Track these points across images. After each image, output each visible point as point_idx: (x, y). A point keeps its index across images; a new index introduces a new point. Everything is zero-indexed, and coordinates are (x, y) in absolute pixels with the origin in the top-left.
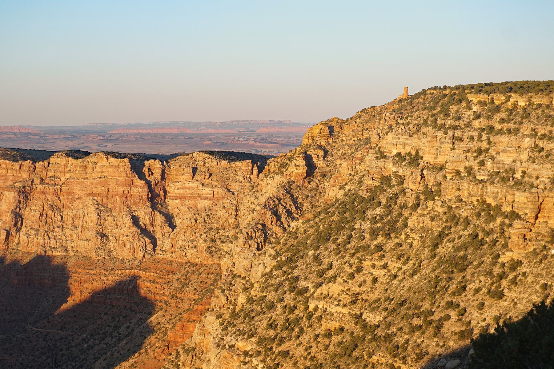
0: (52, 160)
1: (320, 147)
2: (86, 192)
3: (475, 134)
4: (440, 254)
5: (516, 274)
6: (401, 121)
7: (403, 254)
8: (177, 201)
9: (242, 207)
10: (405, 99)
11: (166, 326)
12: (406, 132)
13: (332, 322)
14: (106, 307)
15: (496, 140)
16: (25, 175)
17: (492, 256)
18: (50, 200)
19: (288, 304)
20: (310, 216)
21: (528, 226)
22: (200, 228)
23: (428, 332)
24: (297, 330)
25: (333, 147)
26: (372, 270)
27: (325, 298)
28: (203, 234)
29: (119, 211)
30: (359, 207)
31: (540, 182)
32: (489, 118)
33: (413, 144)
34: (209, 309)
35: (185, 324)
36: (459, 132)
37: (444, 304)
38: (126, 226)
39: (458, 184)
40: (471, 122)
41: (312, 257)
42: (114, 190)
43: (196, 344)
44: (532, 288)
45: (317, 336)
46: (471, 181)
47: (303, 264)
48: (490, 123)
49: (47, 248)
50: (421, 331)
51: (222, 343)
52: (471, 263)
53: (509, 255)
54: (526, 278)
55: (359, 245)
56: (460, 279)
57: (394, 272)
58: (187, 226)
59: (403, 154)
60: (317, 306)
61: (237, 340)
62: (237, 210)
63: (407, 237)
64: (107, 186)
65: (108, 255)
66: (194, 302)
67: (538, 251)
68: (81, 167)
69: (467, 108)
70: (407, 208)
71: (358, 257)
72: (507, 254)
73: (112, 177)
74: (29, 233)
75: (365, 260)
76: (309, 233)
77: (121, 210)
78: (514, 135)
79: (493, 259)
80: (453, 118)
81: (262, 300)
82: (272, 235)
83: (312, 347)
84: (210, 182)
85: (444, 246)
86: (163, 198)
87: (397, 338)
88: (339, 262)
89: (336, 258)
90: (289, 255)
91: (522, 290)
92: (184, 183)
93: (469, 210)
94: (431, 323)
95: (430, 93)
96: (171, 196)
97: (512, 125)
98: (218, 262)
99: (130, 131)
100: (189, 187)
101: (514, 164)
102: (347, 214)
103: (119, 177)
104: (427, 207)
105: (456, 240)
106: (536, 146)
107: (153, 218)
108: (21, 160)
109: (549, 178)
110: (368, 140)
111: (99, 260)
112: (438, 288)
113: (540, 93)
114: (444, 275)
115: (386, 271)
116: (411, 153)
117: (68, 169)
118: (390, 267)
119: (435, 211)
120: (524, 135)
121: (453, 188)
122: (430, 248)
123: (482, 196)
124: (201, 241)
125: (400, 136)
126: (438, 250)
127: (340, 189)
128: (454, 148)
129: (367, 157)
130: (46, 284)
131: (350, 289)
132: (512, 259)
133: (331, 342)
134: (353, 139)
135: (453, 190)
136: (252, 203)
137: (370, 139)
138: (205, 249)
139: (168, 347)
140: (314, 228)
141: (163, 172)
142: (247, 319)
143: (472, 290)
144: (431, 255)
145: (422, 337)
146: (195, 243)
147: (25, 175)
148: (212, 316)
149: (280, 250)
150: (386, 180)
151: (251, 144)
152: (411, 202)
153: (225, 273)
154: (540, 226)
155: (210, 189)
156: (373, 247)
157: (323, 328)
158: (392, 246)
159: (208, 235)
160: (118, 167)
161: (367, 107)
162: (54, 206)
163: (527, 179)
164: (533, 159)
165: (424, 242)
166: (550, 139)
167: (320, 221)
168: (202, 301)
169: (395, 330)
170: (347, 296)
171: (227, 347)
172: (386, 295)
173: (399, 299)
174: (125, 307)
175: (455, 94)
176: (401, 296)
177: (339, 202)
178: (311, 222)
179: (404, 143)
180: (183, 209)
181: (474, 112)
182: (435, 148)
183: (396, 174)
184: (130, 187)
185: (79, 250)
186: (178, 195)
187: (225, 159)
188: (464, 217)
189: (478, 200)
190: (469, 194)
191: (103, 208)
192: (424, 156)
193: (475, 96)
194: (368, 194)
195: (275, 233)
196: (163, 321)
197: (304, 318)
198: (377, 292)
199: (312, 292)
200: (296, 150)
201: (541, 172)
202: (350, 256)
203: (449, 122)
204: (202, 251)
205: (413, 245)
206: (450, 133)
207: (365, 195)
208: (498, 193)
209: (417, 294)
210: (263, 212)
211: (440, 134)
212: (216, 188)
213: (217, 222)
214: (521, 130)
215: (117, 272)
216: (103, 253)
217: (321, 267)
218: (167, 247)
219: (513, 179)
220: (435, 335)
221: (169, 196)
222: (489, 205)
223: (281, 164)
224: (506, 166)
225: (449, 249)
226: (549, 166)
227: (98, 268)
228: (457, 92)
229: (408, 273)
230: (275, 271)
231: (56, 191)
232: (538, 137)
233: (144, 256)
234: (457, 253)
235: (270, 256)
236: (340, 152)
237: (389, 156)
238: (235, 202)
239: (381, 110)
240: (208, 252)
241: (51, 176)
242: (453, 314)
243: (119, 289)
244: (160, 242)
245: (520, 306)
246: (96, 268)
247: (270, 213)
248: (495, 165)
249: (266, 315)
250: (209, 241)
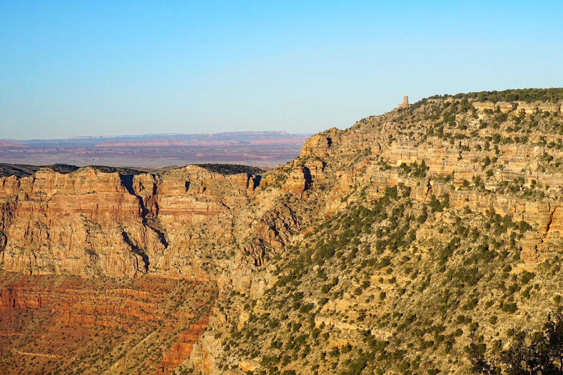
0: (38, 175)
1: (318, 158)
2: (74, 208)
3: (482, 143)
4: (450, 267)
5: (528, 286)
6: (404, 131)
7: (411, 268)
8: (170, 216)
9: (239, 222)
10: (405, 108)
11: (161, 347)
12: (411, 142)
13: (340, 339)
14: (96, 328)
15: (504, 149)
16: (8, 191)
17: (503, 268)
18: (36, 217)
19: (294, 322)
20: (311, 229)
21: (539, 237)
22: (195, 244)
23: (440, 348)
24: (303, 348)
25: (332, 158)
26: (380, 285)
27: (331, 314)
28: (198, 250)
29: (109, 228)
30: (364, 219)
31: (551, 191)
32: (496, 127)
33: (419, 154)
34: (207, 328)
35: (181, 344)
36: (466, 141)
37: (456, 318)
38: (116, 243)
39: (466, 194)
40: (477, 131)
41: (317, 272)
42: (104, 206)
43: (194, 365)
44: (546, 300)
45: (324, 354)
46: (480, 191)
47: (308, 280)
48: (497, 131)
49: (33, 268)
50: (433, 347)
51: (224, 364)
52: (482, 276)
53: (521, 267)
54: (539, 290)
55: (366, 259)
56: (471, 293)
57: (402, 286)
58: (182, 243)
59: (408, 165)
60: (323, 323)
61: (240, 360)
62: (233, 225)
63: (416, 250)
64: (96, 201)
65: (98, 274)
66: (189, 321)
67: (550, 262)
68: (68, 182)
69: (473, 117)
70: (414, 220)
71: (365, 272)
72: (519, 265)
73: (102, 192)
74: (13, 251)
75: (372, 274)
76: (311, 247)
77: (111, 226)
78: (523, 144)
79: (504, 271)
80: (459, 127)
81: (266, 318)
82: (270, 250)
83: (319, 366)
84: (205, 196)
85: (453, 259)
86: (155, 213)
87: (408, 355)
88: (345, 277)
89: (341, 273)
90: (293, 270)
91: (535, 302)
92: (178, 198)
93: (478, 221)
94: (442, 338)
95: (431, 102)
96: (163, 211)
97: (520, 133)
98: (215, 279)
99: (119, 144)
100: (183, 202)
101: (523, 173)
102: (352, 227)
103: (108, 192)
104: (435, 219)
105: (466, 252)
106: (546, 154)
107: (144, 234)
108: (5, 175)
109: (560, 187)
110: (368, 151)
111: (88, 279)
112: (449, 302)
113: (547, 101)
114: (455, 289)
115: (394, 285)
116: (417, 163)
117: (55, 185)
118: (399, 281)
119: (443, 223)
120: (532, 144)
121: (461, 198)
122: (439, 261)
123: (491, 206)
124: (196, 258)
125: (405, 146)
126: (448, 263)
127: (342, 202)
128: (460, 158)
129: (370, 168)
130: (32, 305)
131: (357, 305)
132: (524, 272)
133: (338, 360)
134: (352, 150)
135: (462, 201)
136: (248, 217)
137: (370, 149)
138: (200, 265)
139: (163, 370)
140: (316, 242)
141: (155, 187)
142: (250, 337)
143: (484, 304)
144: (440, 268)
145: (434, 354)
146: (190, 260)
147: (8, 191)
148: (210, 335)
149: (281, 265)
150: (391, 192)
151: (245, 157)
152: (418, 214)
153: (222, 291)
154: (552, 236)
155: (204, 204)
156: (380, 261)
157: (330, 346)
158: (400, 259)
159: (204, 252)
160: (108, 181)
161: (366, 116)
162: (40, 224)
163: (537, 188)
164: (543, 168)
165: (432, 254)
166: (559, 147)
167: (322, 235)
168: (198, 320)
169: (406, 346)
170: (355, 312)
171: (230, 367)
172: (395, 310)
173: (409, 314)
174: (117, 329)
175: (458, 103)
176: (411, 311)
177: (342, 215)
178: (313, 236)
179: (410, 153)
180: (176, 224)
181: (481, 121)
182: (442, 158)
183: (402, 185)
184: (120, 202)
185: (67, 269)
186: (171, 210)
187: (219, 172)
188: (473, 228)
189: (487, 211)
190: (478, 205)
191: (92, 225)
192: (430, 166)
193: (482, 104)
194: (373, 206)
195: (274, 248)
196: (157, 341)
197: (311, 336)
198: (386, 308)
199: (317, 308)
200: (294, 162)
201: (551, 181)
202: (356, 271)
203: (456, 131)
204: (197, 268)
205: (422, 258)
206: (457, 142)
207: (370, 207)
208: (507, 203)
209: (427, 309)
210: (261, 226)
211: (446, 143)
212: (211, 202)
213: (213, 237)
214: (530, 139)
215: (107, 291)
216: (93, 271)
217: (327, 283)
218: (161, 264)
219: (523, 189)
220: (448, 351)
221: (161, 212)
222: (498, 216)
223: (278, 177)
224: (515, 176)
225: (459, 262)
226: (559, 175)
227: (87, 287)
228: (460, 100)
229: (417, 287)
230: (278, 287)
231: (43, 207)
232: (548, 146)
233: (136, 274)
234: (467, 266)
235: (271, 272)
236: (340, 164)
237: (394, 167)
238: (231, 216)
239: (381, 120)
240: (203, 269)
241: (37, 191)
242: (465, 328)
243: (110, 309)
244: (153, 259)
245: (534, 319)
246: (85, 287)
247: (268, 228)
248: (504, 175)
249: (270, 334)
250: (204, 257)
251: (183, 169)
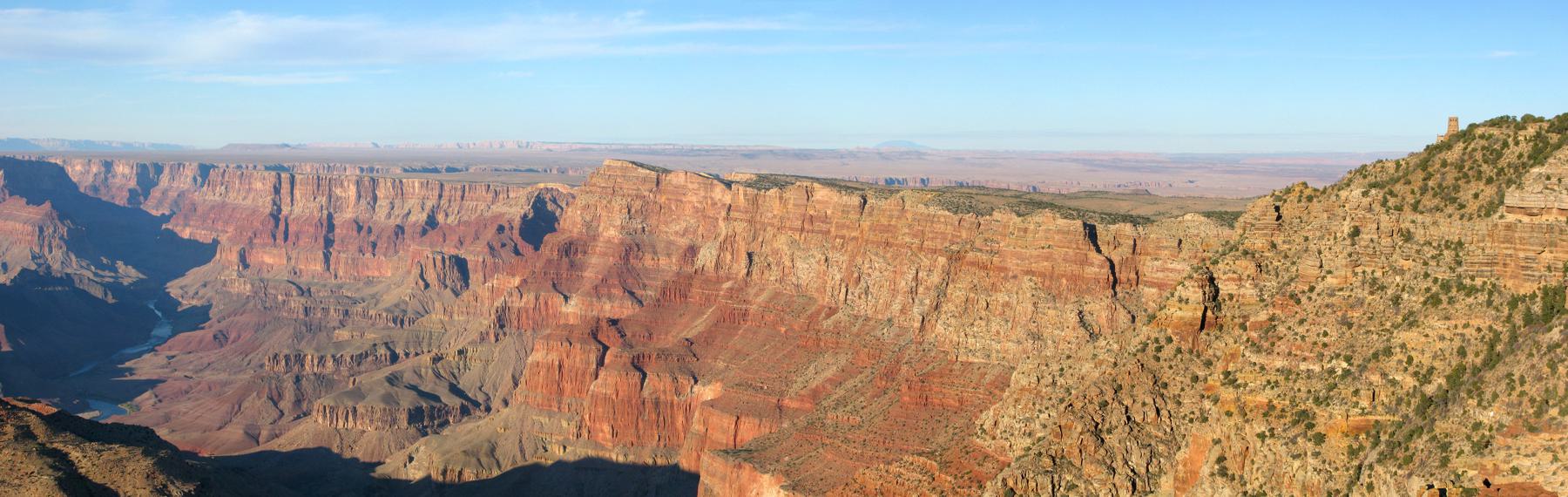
86: (1134, 283)
103: (1068, 248)
251: (1180, 219)
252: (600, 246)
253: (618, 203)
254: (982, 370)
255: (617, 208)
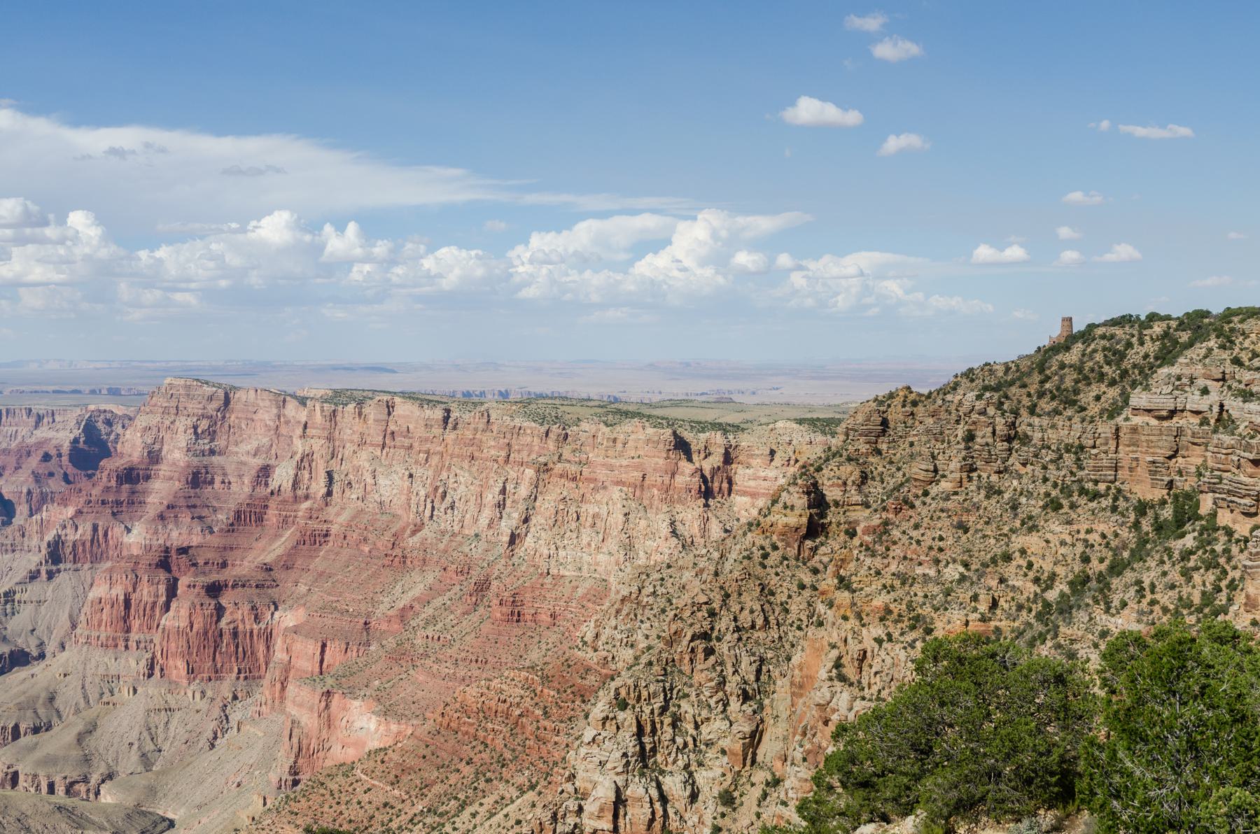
252: (163, 469)
253: (183, 423)
254: (574, 583)
255: (181, 429)
